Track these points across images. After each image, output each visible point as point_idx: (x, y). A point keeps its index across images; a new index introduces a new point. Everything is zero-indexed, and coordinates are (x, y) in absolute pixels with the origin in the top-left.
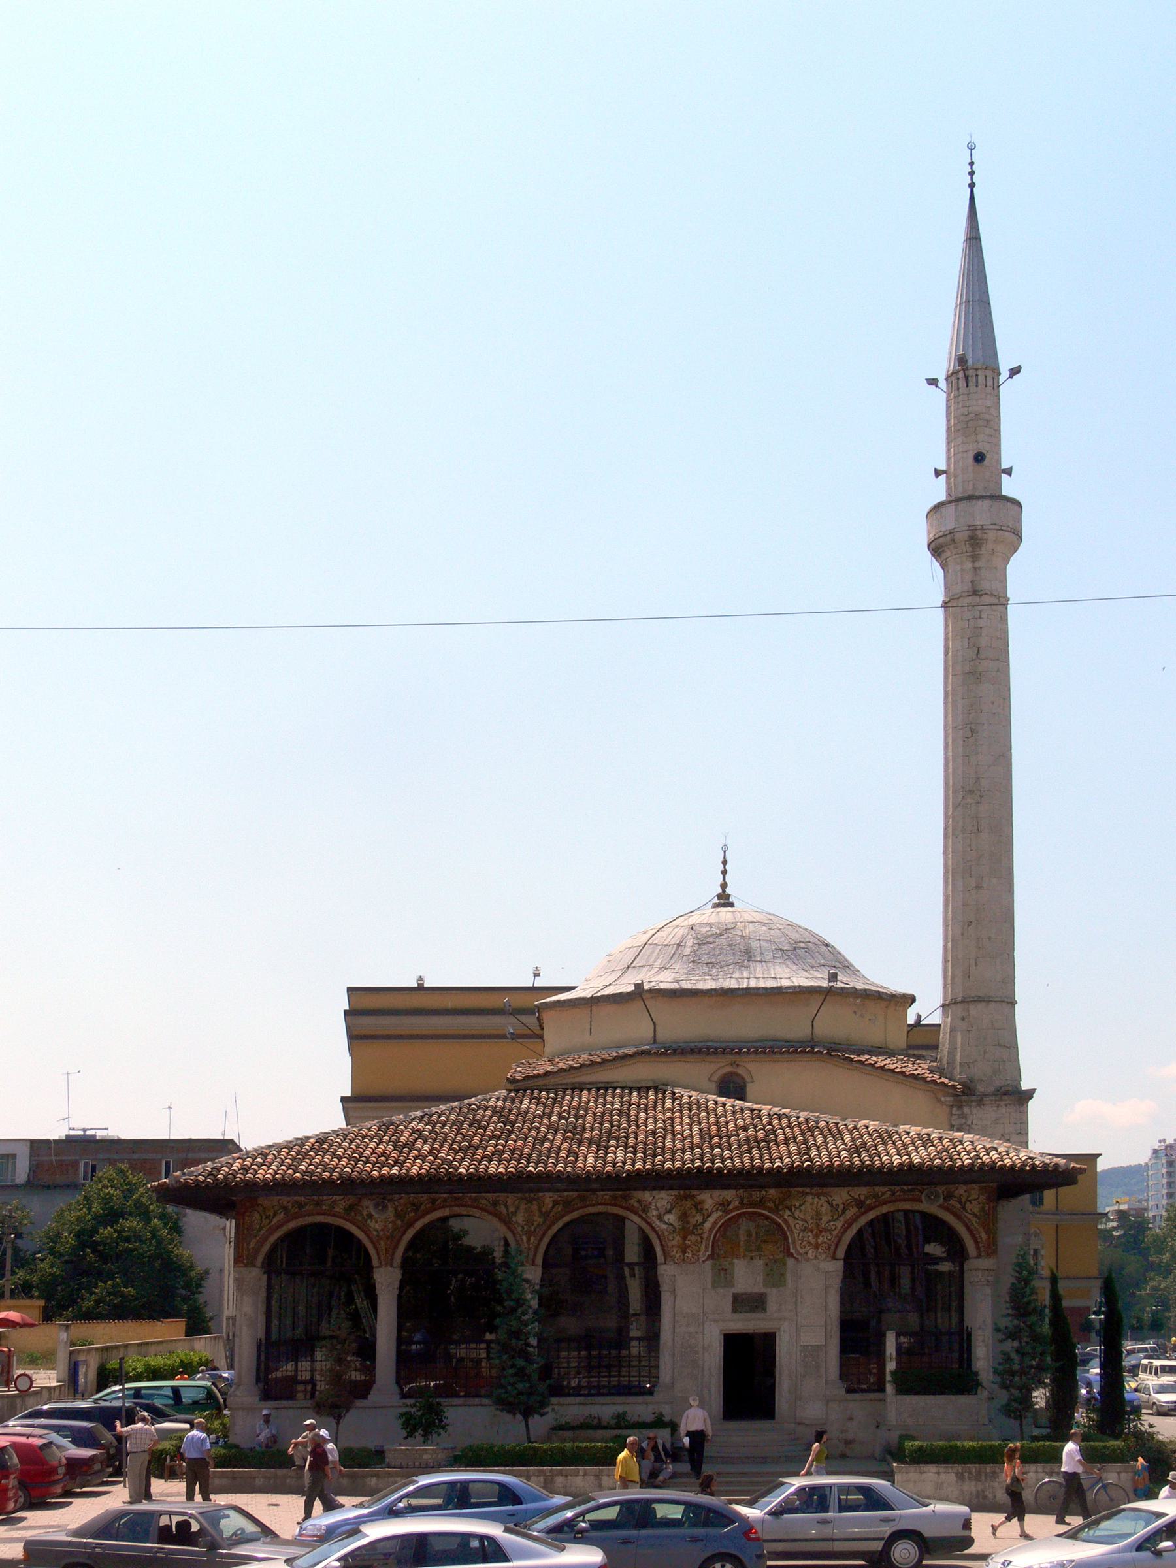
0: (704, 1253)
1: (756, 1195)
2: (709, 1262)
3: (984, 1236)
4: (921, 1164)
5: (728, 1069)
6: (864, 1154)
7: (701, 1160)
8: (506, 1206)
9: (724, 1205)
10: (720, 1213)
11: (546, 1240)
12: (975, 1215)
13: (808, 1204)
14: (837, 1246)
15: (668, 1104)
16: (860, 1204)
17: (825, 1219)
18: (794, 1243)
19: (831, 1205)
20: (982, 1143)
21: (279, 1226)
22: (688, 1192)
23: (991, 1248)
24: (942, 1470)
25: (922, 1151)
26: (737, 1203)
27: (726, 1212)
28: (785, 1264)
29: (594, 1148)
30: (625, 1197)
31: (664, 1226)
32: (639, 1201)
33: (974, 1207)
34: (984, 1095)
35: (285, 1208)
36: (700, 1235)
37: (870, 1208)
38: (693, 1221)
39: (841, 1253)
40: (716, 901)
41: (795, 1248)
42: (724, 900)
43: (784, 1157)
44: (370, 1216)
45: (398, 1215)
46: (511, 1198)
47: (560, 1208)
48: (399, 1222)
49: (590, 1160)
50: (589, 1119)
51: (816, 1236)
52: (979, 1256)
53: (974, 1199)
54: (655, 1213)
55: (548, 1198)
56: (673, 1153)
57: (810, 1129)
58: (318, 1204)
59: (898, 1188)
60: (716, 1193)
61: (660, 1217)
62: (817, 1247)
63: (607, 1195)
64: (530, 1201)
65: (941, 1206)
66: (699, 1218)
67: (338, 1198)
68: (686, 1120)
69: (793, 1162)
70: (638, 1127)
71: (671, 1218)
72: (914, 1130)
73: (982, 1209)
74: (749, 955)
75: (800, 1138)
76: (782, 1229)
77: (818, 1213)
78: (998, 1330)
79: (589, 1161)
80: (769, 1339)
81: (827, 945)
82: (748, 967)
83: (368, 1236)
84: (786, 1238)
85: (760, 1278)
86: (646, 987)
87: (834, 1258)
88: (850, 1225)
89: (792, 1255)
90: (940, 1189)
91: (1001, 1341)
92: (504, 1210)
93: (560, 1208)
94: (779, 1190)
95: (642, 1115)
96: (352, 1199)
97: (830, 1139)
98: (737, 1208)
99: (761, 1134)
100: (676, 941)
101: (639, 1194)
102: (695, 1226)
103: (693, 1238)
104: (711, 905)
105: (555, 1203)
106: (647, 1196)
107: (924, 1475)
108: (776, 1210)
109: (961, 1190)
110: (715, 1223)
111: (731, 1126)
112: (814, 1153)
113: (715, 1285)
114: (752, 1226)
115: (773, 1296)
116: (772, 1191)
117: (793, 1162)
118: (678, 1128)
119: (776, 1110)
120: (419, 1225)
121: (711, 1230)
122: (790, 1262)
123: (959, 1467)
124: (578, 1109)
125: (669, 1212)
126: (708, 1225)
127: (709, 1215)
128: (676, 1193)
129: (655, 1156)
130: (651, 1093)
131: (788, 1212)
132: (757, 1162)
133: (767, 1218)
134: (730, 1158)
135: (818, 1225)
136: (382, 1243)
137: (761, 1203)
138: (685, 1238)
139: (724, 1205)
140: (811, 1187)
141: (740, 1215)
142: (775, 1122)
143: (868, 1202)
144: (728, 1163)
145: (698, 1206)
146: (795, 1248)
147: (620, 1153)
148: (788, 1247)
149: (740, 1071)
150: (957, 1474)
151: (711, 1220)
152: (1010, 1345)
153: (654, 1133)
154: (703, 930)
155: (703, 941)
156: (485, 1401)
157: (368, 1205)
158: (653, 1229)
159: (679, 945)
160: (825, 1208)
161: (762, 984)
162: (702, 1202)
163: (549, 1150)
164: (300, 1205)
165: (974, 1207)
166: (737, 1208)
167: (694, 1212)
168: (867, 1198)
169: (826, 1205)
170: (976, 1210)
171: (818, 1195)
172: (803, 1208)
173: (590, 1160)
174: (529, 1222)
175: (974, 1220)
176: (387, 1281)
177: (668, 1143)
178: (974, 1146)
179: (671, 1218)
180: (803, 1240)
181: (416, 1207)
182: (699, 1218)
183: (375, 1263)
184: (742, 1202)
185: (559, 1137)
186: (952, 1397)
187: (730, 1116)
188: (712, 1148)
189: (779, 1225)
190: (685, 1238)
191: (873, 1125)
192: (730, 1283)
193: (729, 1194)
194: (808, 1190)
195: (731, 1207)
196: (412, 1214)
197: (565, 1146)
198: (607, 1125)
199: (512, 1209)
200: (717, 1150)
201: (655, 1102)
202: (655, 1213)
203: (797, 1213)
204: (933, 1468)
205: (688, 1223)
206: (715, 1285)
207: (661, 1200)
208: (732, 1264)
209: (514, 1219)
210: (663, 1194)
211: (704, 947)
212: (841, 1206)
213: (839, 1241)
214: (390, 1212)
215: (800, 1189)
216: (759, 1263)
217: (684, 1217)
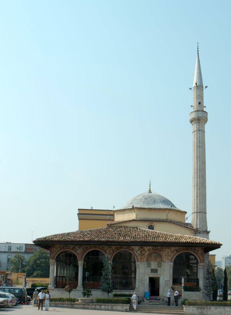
0: (145, 260)
1: (156, 248)
2: (146, 262)
3: (202, 258)
4: (189, 242)
5: (150, 224)
6: (178, 240)
7: (145, 239)
8: (105, 249)
9: (149, 250)
11: (113, 256)
12: (200, 253)
14: (172, 259)
15: (138, 230)
16: (177, 250)
17: (170, 253)
18: (163, 258)
19: (171, 251)
20: (201, 238)
21: (59, 251)
23: (203, 261)
24: (194, 307)
25: (190, 240)
26: (152, 250)
28: (161, 263)
29: (123, 237)
31: (137, 254)
33: (200, 252)
35: (60, 247)
36: (144, 256)
37: (179, 252)
38: (143, 253)
40: (148, 192)
42: (150, 192)
43: (162, 240)
44: (77, 250)
45: (83, 249)
46: (106, 247)
47: (116, 249)
48: (83, 251)
49: (122, 239)
50: (123, 232)
51: (168, 257)
52: (201, 262)
53: (200, 251)
54: (135, 251)
55: (114, 247)
56: (139, 238)
57: (167, 235)
58: (67, 247)
59: (184, 248)
60: (148, 247)
61: (136, 252)
62: (168, 259)
63: (125, 247)
64: (110, 247)
65: (192, 252)
66: (144, 252)
67: (71, 245)
68: (142, 233)
69: (163, 241)
70: (132, 234)
71: (138, 252)
72: (188, 236)
73: (201, 253)
74: (155, 202)
75: (164, 237)
76: (161, 256)
78: (205, 278)
79: (122, 239)
80: (158, 279)
81: (170, 201)
82: (154, 204)
83: (77, 254)
86: (135, 207)
87: (171, 262)
88: (175, 255)
89: (163, 261)
90: (193, 248)
91: (205, 280)
92: (104, 249)
93: (116, 249)
94: (160, 247)
95: (133, 232)
96: (74, 246)
97: (171, 237)
98: (152, 251)
99: (157, 236)
100: (140, 199)
101: (132, 247)
102: (143, 254)
104: (147, 193)
105: (115, 248)
106: (134, 247)
107: (190, 308)
108: (160, 251)
109: (197, 249)
111: (151, 235)
112: (167, 239)
113: (147, 267)
115: (159, 269)
117: (163, 241)
118: (140, 234)
119: (160, 232)
121: (147, 255)
122: (163, 262)
123: (197, 307)
124: (120, 230)
126: (146, 254)
128: (139, 247)
129: (135, 239)
130: (135, 228)
132: (156, 240)
133: (158, 253)
134: (150, 239)
135: (168, 255)
136: (80, 255)
137: (157, 250)
138: (141, 256)
140: (167, 246)
141: (152, 252)
142: (160, 234)
143: (178, 250)
144: (150, 240)
145: (144, 250)
147: (128, 238)
149: (153, 225)
150: (197, 308)
151: (147, 253)
152: (207, 281)
153: (135, 235)
154: (146, 197)
155: (146, 199)
156: (100, 290)
157: (77, 247)
158: (135, 254)
159: (141, 199)
160: (170, 251)
161: (157, 207)
162: (145, 249)
163: (114, 237)
164: (63, 247)
165: (200, 252)
166: (152, 251)
167: (143, 251)
168: (178, 249)
169: (170, 251)
170: (200, 253)
171: (168, 248)
173: (122, 239)
175: (200, 255)
176: (81, 264)
177: (138, 237)
178: (200, 239)
181: (87, 248)
182: (144, 252)
183: (78, 260)
185: (116, 235)
186: (195, 292)
187: (150, 233)
188: (147, 238)
189: (160, 255)
190: (141, 256)
191: (179, 235)
192: (150, 267)
193: (150, 248)
194: (166, 247)
195: (151, 250)
196: (86, 249)
197: (117, 236)
198: (126, 233)
199: (106, 249)
200: (148, 238)
201: (136, 230)
202: (135, 251)
204: (192, 306)
206: (147, 267)
207: (136, 248)
208: (151, 262)
209: (107, 251)
210: (137, 247)
211: (146, 200)
212: (173, 251)
213: (173, 258)
214: (82, 249)
216: (156, 263)
217: (141, 252)
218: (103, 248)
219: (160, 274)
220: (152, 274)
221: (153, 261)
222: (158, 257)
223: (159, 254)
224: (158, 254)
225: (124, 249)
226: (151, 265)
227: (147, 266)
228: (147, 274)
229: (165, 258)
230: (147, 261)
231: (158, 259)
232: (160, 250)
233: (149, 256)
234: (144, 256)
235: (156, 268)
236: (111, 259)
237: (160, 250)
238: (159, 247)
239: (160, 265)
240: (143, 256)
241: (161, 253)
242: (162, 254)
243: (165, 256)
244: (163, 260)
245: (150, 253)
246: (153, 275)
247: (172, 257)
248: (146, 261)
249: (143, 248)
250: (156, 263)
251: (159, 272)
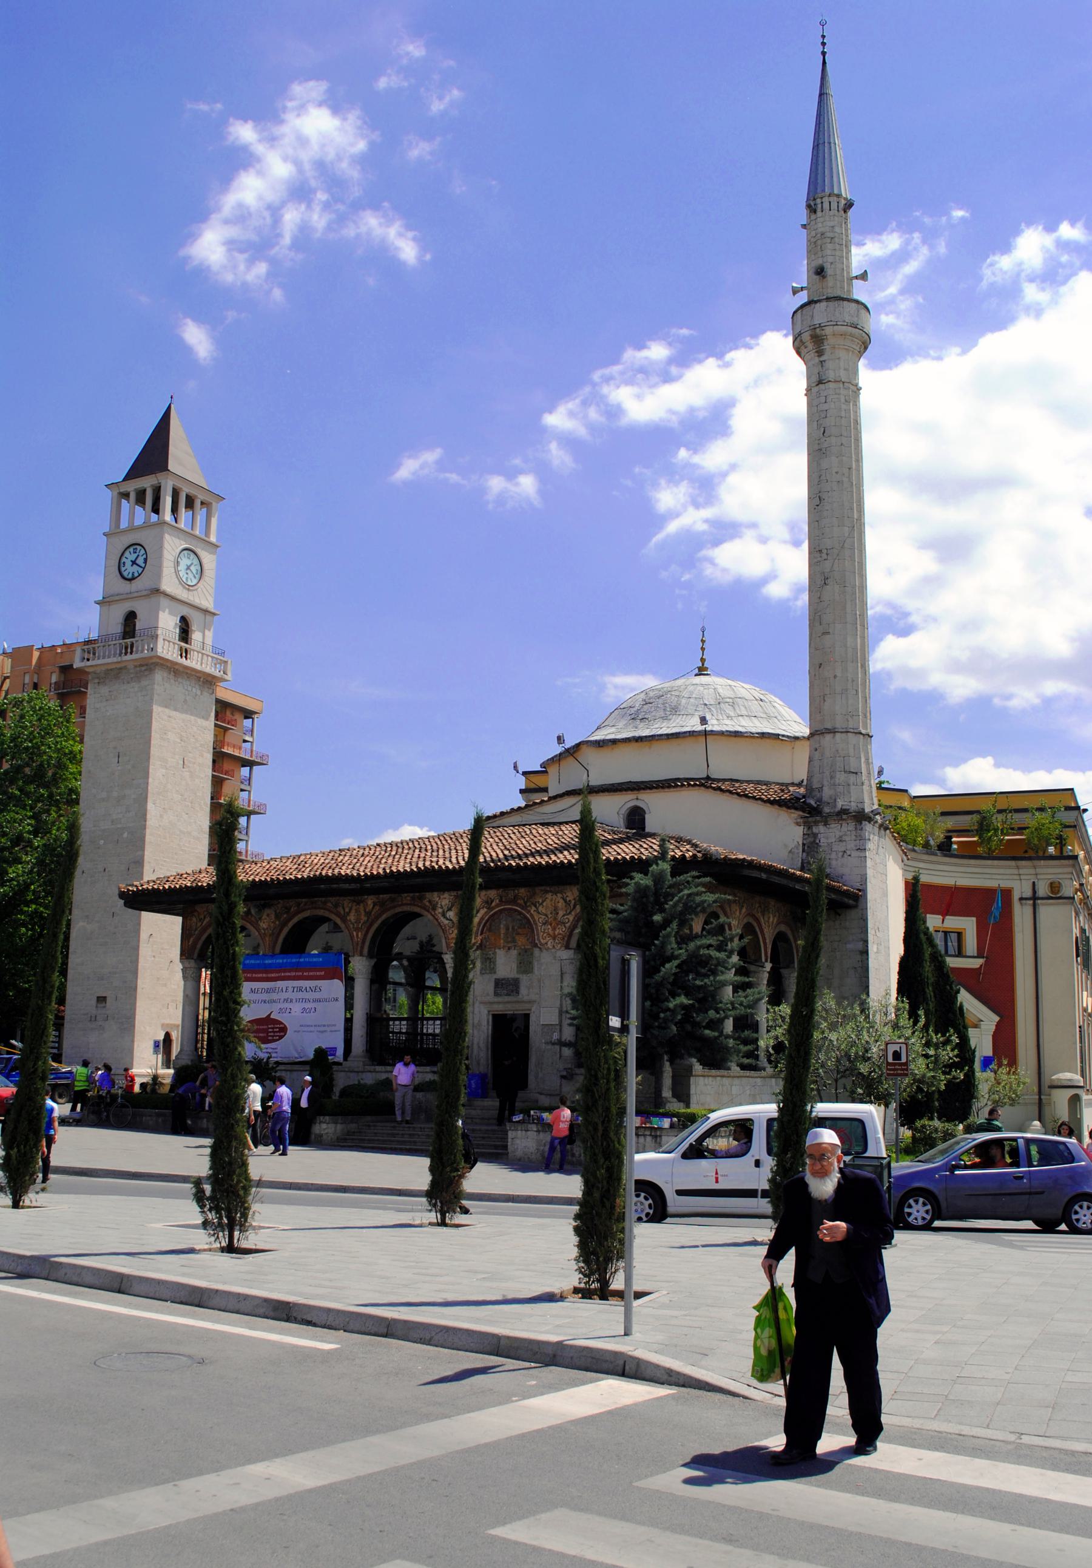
1: (511, 894)
13: (548, 901)
17: (561, 913)
19: (565, 901)
27: (490, 909)
30: (421, 898)
32: (430, 901)
34: (829, 815)
39: (573, 943)
45: (277, 917)
46: (346, 902)
51: (554, 929)
54: (440, 910)
55: (370, 901)
61: (444, 915)
62: (554, 939)
63: (407, 897)
64: (358, 903)
71: (451, 914)
77: (556, 909)
80: (527, 1017)
84: (533, 931)
85: (514, 966)
87: (567, 947)
89: (536, 945)
93: (377, 908)
98: (497, 906)
101: (428, 895)
105: (375, 904)
106: (435, 896)
108: (525, 907)
110: (482, 919)
115: (524, 979)
116: (522, 890)
120: (290, 924)
121: (479, 923)
122: (536, 951)
125: (450, 909)
128: (455, 893)
131: (534, 908)
133: (520, 913)
135: (555, 919)
137: (514, 901)
141: (501, 911)
160: (561, 904)
166: (497, 906)
169: (561, 901)
174: (358, 921)
179: (451, 914)
184: (501, 901)
192: (493, 970)
199: (347, 910)
203: (540, 909)
208: (495, 953)
210: (446, 895)
218: (336, 906)
219: (526, 998)
220: (500, 999)
223: (526, 917)
225: (402, 905)
226: (494, 963)
227: (482, 969)
228: (481, 1003)
229: (543, 933)
231: (521, 940)
232: (525, 903)
235: (517, 976)
236: (362, 948)
237: (525, 903)
238: (522, 891)
239: (526, 964)
242: (532, 915)
243: (544, 924)
245: (493, 915)
246: (506, 1006)
247: (567, 925)
251: (523, 991)
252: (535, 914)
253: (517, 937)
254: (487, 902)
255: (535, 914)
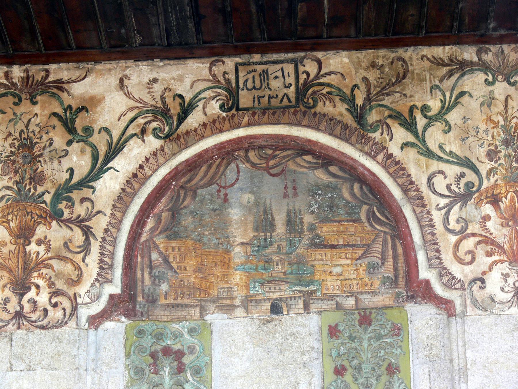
0: (95, 292)
2: (116, 327)
9: (169, 118)
10: (153, 143)
13: (471, 104)
18: (431, 243)
22: (36, 71)
26: (214, 108)
27: (174, 138)
28: (398, 331)
36: (82, 224)
38: (55, 172)
41: (436, 261)
60: (140, 74)
89: (423, 292)
94: (365, 56)
98: (214, 126)
102: (64, 191)
103: (56, 233)
108: (358, 126)
110: (137, 178)
114: (271, 187)
121: (123, 200)
122: (421, 318)
126: (109, 185)
127: (114, 150)
131: (401, 134)
133: (326, 159)
137: (303, 104)
138: (24, 235)
139: (169, 118)
140: (482, 40)
141: (227, 153)
145: (72, 121)
146: (436, 261)
148: (411, 265)
151: (124, 165)
167: (59, 138)
172: (454, 117)
180: (463, 234)
182: (79, 161)
184: (232, 104)
190: (24, 235)
193: (186, 77)
194: (469, 53)
195: (194, 120)
203: (435, 137)
205: (37, 179)
208: (202, 330)
215: (441, 52)
216: (306, 327)
221: (249, 303)
222: (328, 231)
223: (354, 173)
224: (321, 176)
230: (124, 304)
231: (337, 272)
232: (359, 116)
233: (175, 212)
234: (82, 224)
237: (359, 116)
240: (57, 216)
241: (377, 150)
244: (425, 273)
245: (192, 166)
248: (117, 306)
249: (60, 85)
250: (306, 327)
252: (411, 160)
253: (319, 260)
254: (162, 112)
255: (411, 160)
